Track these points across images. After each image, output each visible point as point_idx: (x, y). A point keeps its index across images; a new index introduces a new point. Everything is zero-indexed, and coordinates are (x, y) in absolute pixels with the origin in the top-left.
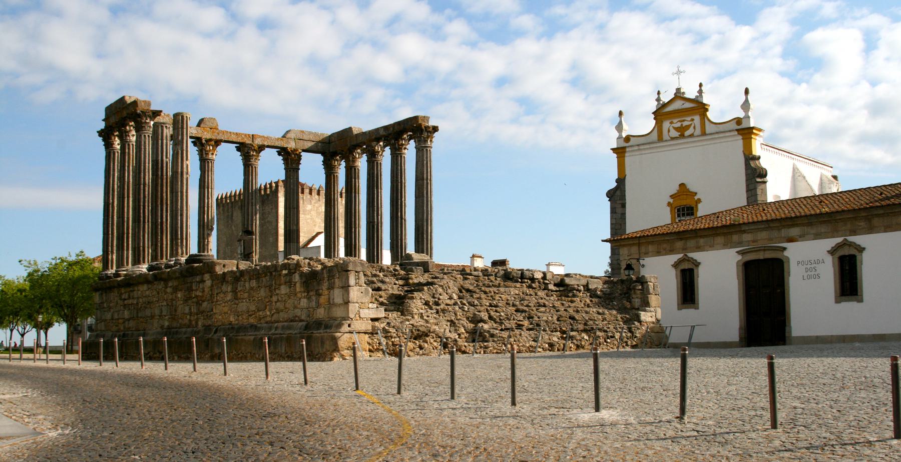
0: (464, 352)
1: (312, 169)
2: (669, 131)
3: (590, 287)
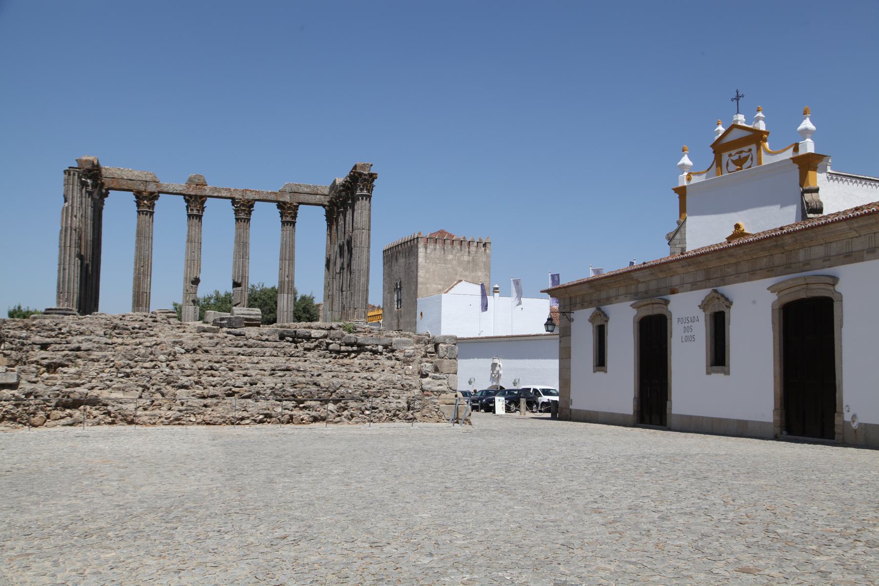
0: (131, 422)
1: (312, 221)
3: (394, 347)
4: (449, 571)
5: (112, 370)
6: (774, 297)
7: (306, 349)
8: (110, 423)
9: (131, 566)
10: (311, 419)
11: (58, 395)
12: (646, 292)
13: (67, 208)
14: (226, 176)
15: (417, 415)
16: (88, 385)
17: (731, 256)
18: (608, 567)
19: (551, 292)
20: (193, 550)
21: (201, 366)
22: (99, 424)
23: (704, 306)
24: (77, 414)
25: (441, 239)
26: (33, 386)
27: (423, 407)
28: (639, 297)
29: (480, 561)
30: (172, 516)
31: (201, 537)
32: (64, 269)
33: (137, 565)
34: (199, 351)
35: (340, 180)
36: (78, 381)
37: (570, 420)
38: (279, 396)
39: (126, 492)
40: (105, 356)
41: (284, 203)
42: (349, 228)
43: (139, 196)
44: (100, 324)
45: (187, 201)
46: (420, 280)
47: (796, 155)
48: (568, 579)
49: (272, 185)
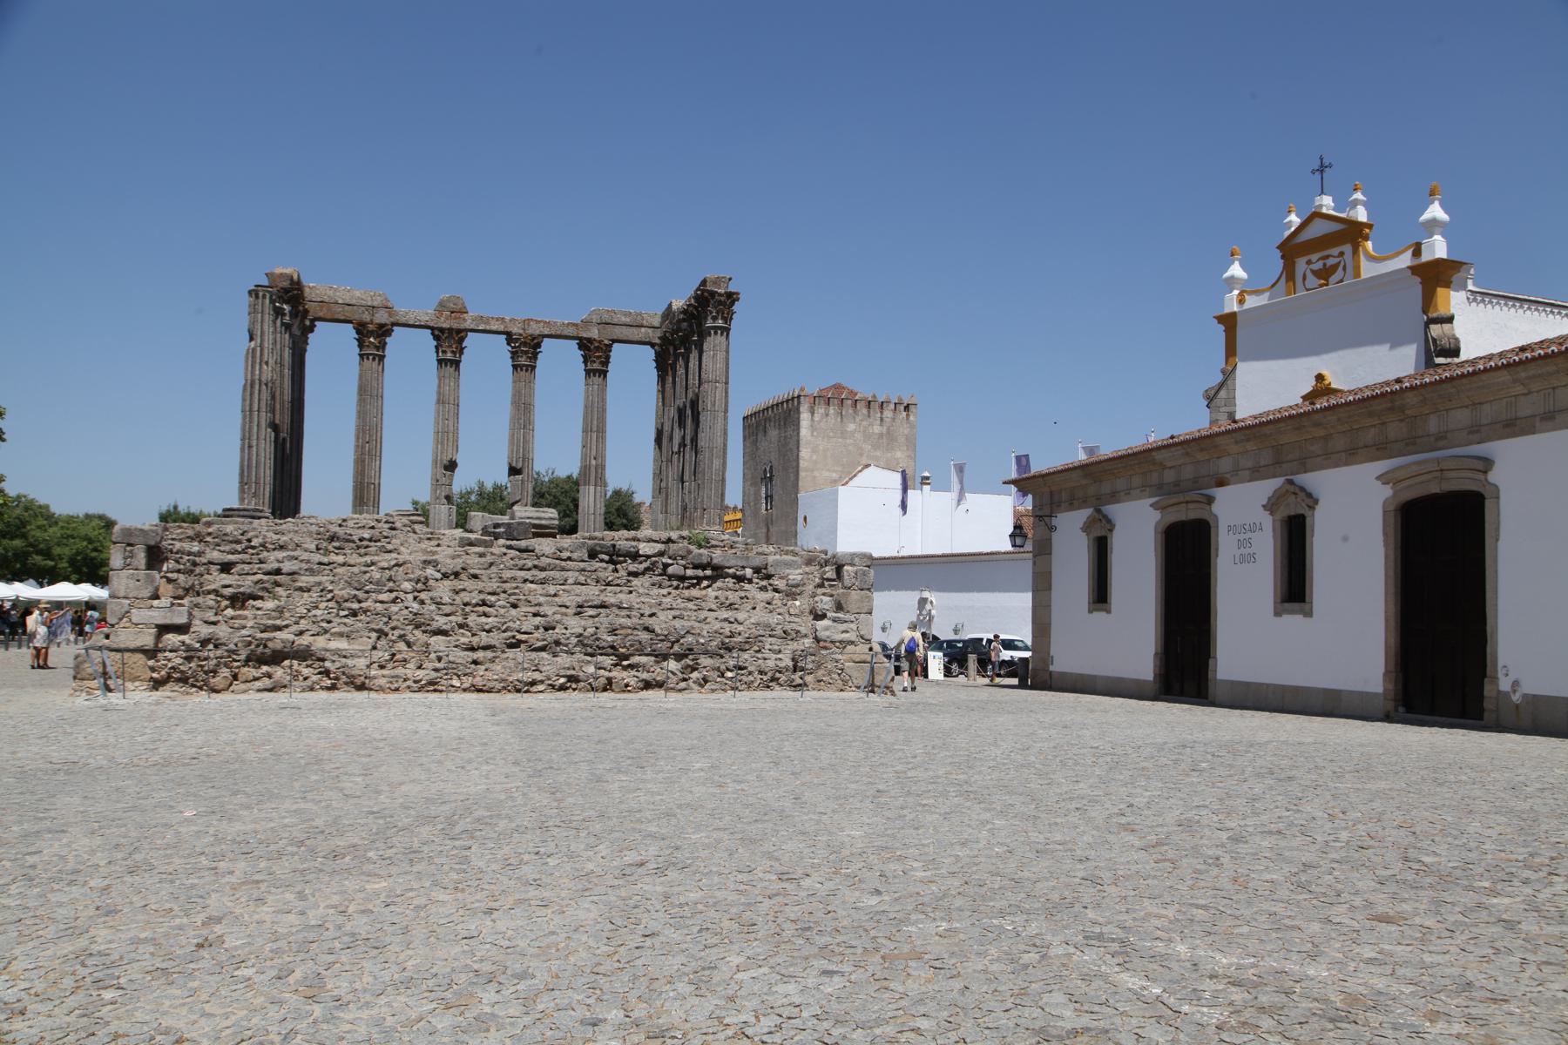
0: (361, 688)
1: (634, 369)
2: (1304, 278)
3: (771, 570)
4: (913, 917)
5: (331, 604)
6: (1387, 491)
7: (630, 574)
8: (328, 689)
9: (415, 902)
10: (641, 685)
11: (250, 643)
12: (1177, 484)
13: (254, 350)
14: (498, 299)
15: (809, 679)
16: (295, 628)
17: (1317, 425)
18: (1164, 912)
19: (1024, 484)
20: (505, 880)
21: (467, 599)
22: (312, 689)
23: (1271, 507)
24: (279, 672)
25: (837, 398)
26: (212, 629)
27: (819, 667)
28: (1165, 492)
29: (959, 902)
30: (458, 829)
31: (512, 861)
32: (250, 447)
33: (423, 901)
34: (463, 576)
35: (678, 304)
36: (278, 622)
37: (1050, 688)
38: (590, 647)
39: (379, 792)
40: (319, 584)
41: (590, 340)
42: (693, 380)
43: (362, 330)
44: (310, 533)
45: (436, 338)
46: (802, 464)
47: (1416, 262)
48: (1105, 930)
49: (570, 310)
